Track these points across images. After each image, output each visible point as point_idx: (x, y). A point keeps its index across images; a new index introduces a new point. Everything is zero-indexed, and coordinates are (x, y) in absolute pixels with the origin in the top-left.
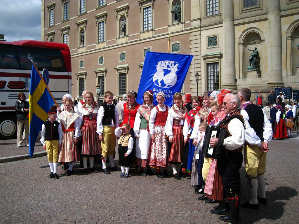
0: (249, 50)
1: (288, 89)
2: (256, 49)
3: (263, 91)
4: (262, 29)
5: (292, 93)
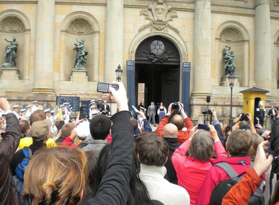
0: (6, 40)
1: (75, 99)
2: (15, 40)
3: (30, 99)
4: (27, 15)
5: (80, 103)
